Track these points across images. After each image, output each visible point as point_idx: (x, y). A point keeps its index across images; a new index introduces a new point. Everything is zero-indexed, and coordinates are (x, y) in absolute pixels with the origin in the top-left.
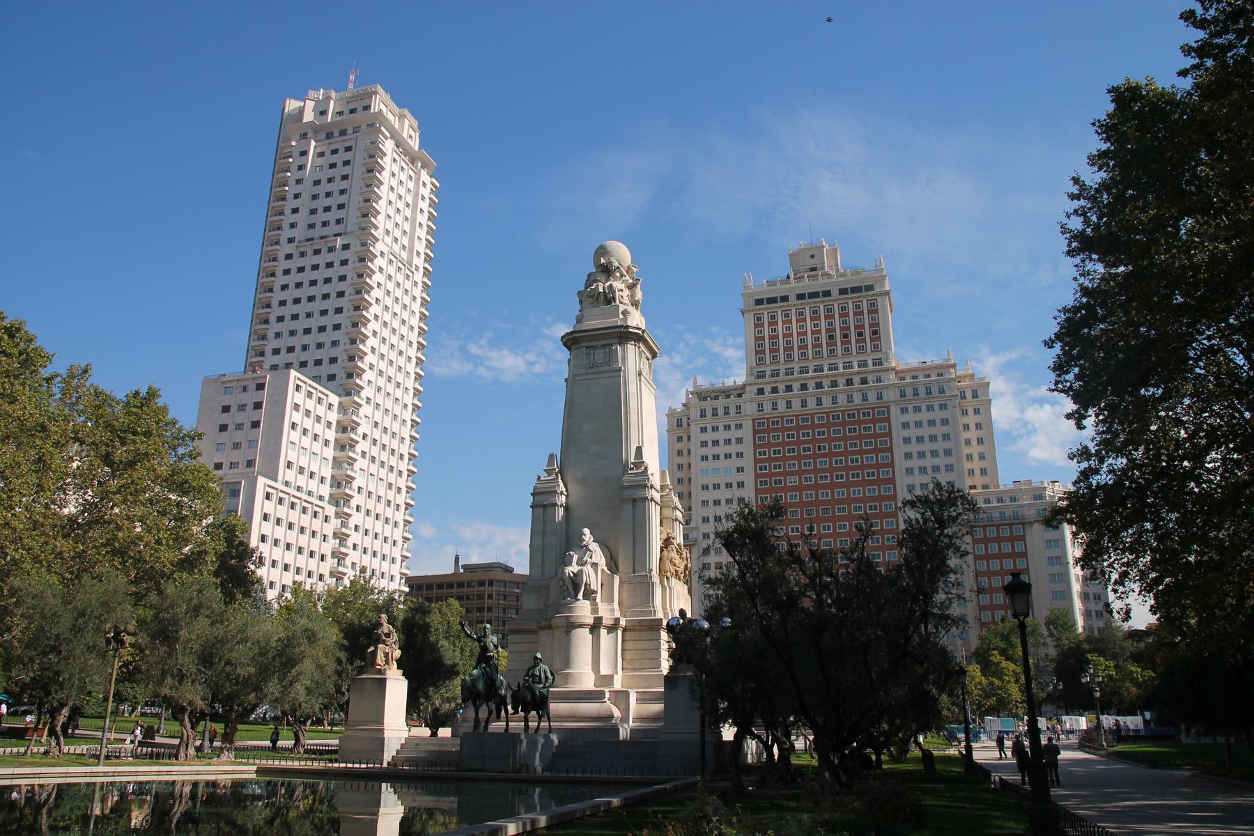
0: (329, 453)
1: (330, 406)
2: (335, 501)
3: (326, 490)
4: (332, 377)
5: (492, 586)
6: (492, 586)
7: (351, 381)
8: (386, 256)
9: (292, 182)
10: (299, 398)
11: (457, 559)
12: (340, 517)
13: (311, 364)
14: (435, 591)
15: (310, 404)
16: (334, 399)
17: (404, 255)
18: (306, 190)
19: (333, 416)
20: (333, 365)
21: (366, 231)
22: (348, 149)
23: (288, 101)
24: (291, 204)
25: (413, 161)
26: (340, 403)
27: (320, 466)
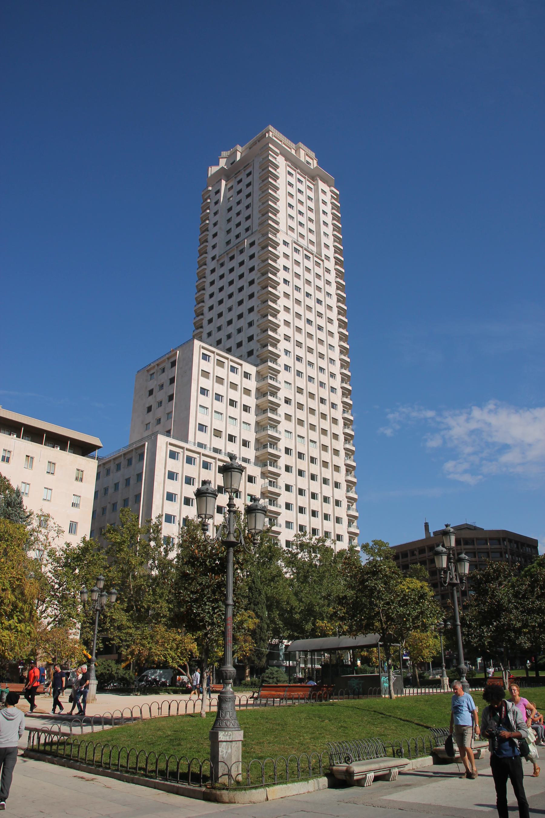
0: (251, 417)
1: (247, 375)
2: (261, 462)
3: (250, 453)
4: (250, 353)
5: (460, 545)
6: (460, 545)
7: (265, 349)
8: (290, 245)
9: (212, 215)
10: (207, 366)
11: (427, 526)
12: (267, 477)
13: (234, 348)
14: (409, 558)
15: (222, 372)
16: (252, 369)
17: (314, 249)
18: (221, 218)
19: (252, 384)
20: (251, 343)
21: (266, 224)
22: (249, 174)
23: (210, 168)
24: (213, 231)
25: (313, 178)
26: (258, 373)
27: (240, 430)
